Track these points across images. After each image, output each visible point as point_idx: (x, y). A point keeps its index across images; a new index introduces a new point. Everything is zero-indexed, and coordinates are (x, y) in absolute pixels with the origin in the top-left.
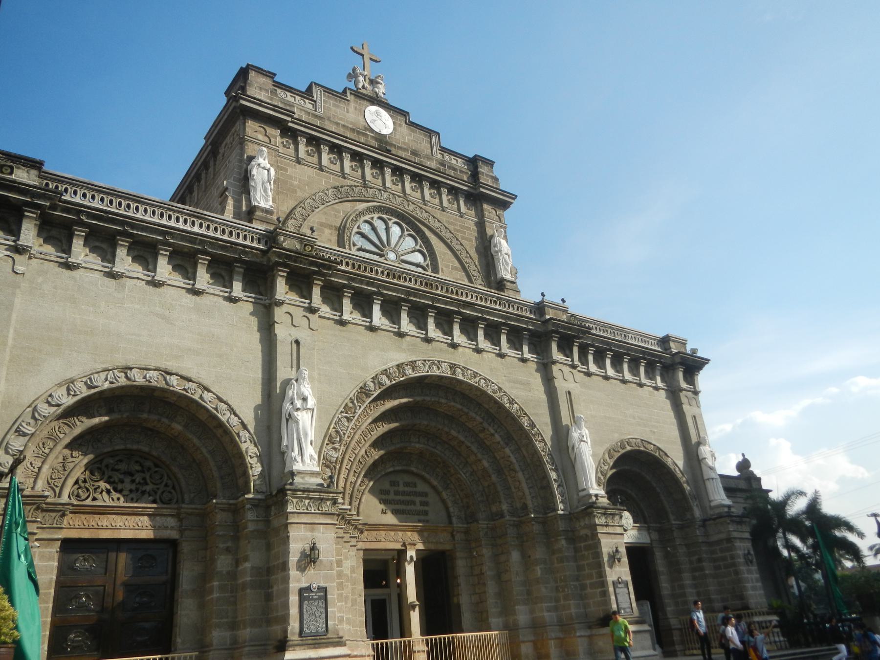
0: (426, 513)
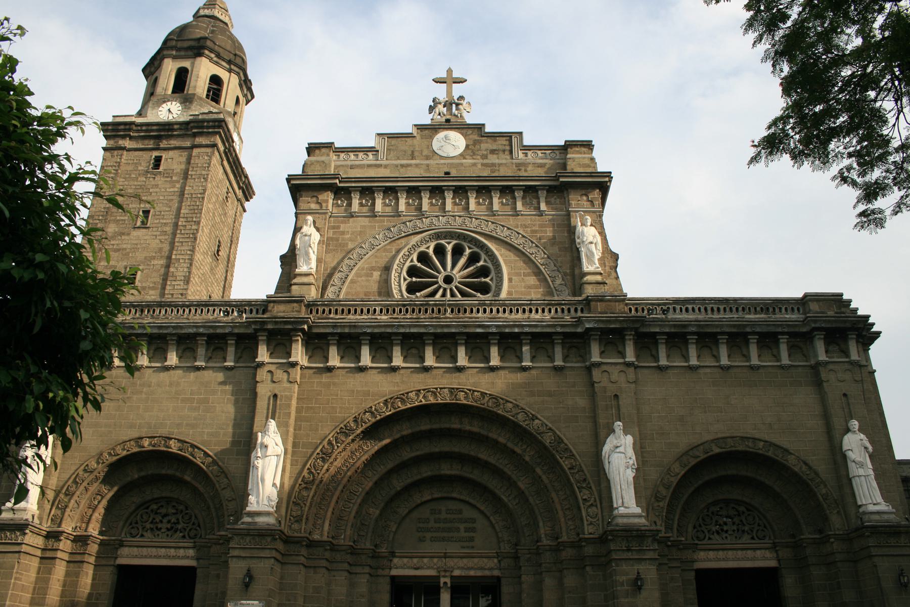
0: (472, 539)
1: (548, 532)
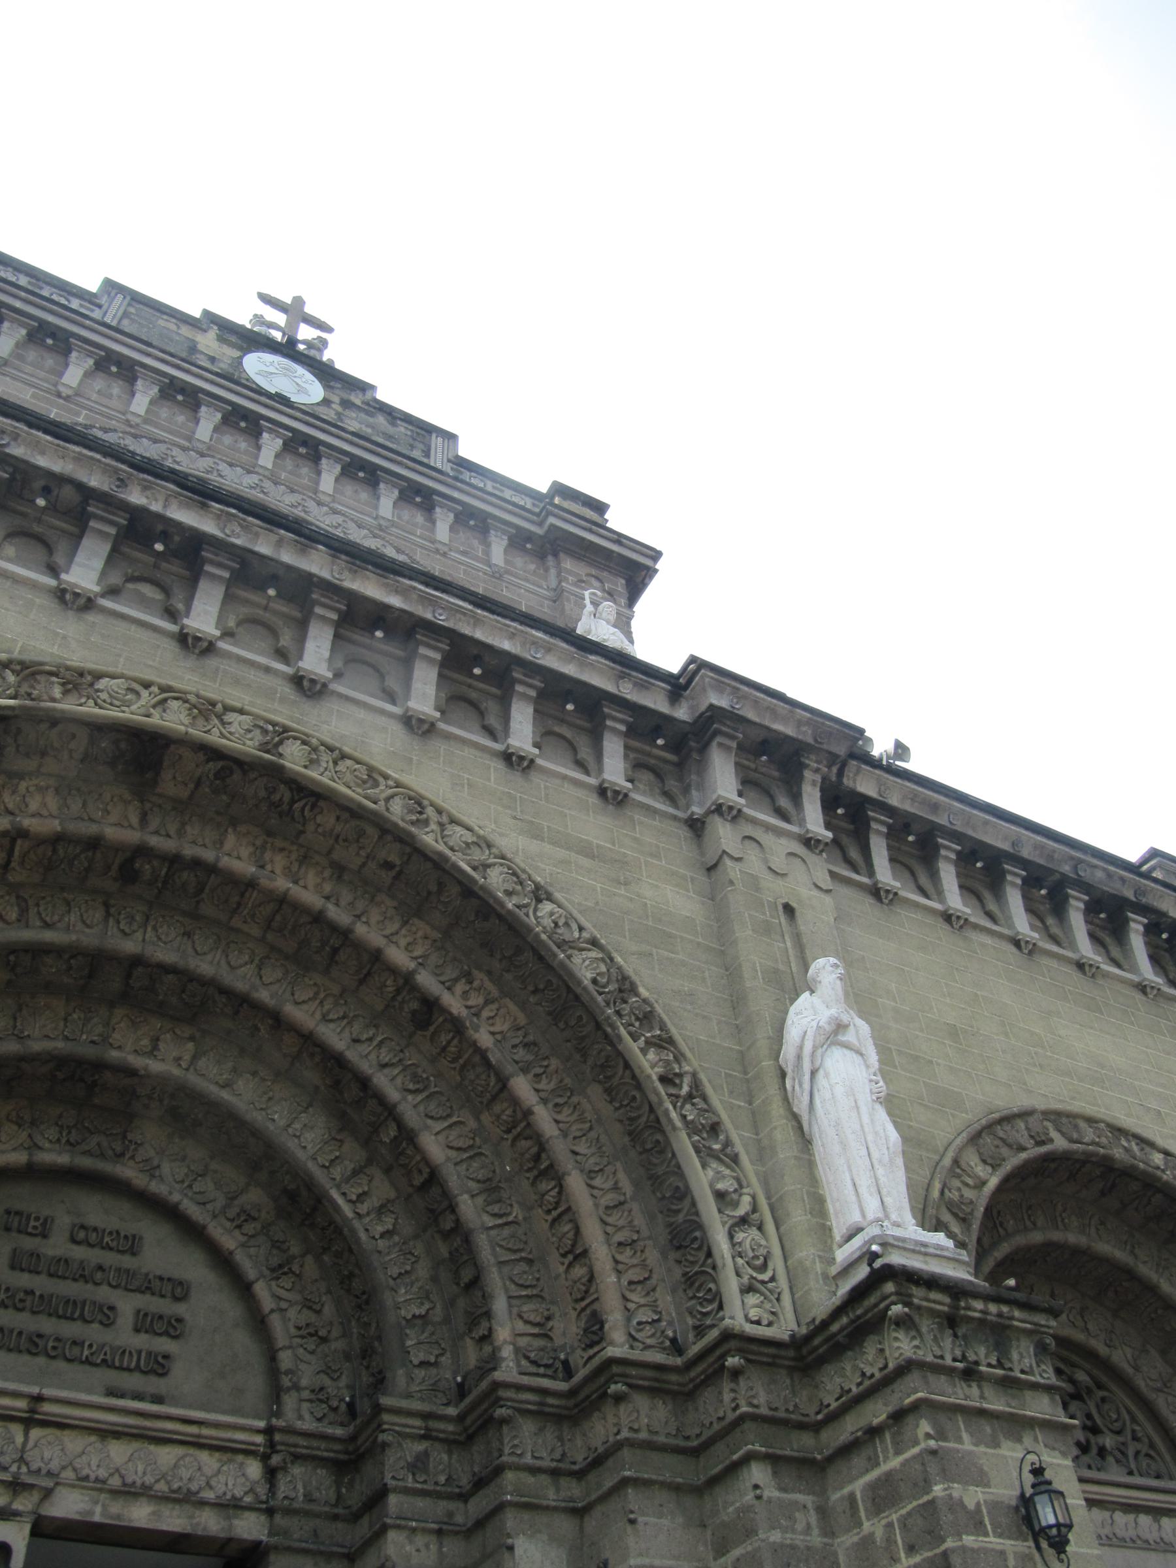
0: (159, 1366)
1: (523, 1342)
